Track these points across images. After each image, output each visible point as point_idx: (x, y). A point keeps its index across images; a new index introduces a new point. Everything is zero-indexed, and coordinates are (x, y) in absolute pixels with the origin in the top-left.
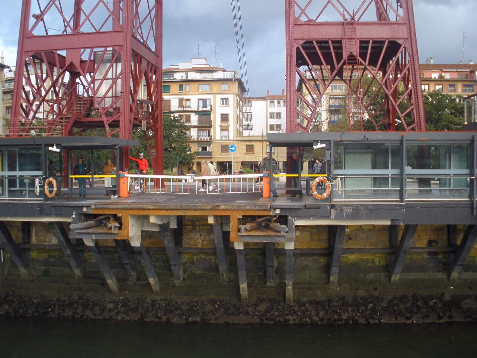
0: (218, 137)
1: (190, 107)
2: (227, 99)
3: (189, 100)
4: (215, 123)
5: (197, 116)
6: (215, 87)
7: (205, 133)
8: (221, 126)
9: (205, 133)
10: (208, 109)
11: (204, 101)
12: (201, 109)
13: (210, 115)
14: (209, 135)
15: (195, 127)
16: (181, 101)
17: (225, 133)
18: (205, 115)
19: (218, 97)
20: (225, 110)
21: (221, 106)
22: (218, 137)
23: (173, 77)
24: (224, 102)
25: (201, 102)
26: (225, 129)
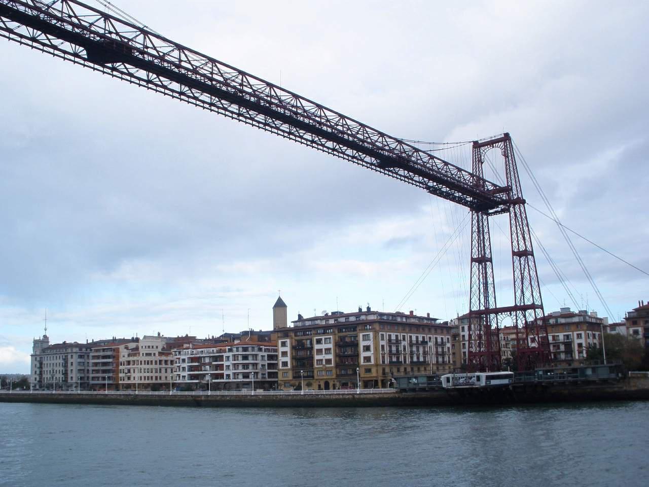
0: (577, 357)
1: (559, 340)
2: (581, 334)
3: (558, 336)
4: (575, 349)
5: (563, 345)
6: (573, 328)
7: (569, 355)
8: (578, 350)
9: (569, 355)
10: (570, 340)
11: (568, 336)
12: (566, 341)
13: (571, 344)
14: (572, 356)
15: (562, 352)
16: (554, 337)
17: (581, 355)
18: (568, 345)
19: (575, 333)
20: (579, 341)
21: (577, 339)
22: (577, 357)
23: (549, 321)
24: (579, 336)
25: (566, 338)
26: (580, 352)
